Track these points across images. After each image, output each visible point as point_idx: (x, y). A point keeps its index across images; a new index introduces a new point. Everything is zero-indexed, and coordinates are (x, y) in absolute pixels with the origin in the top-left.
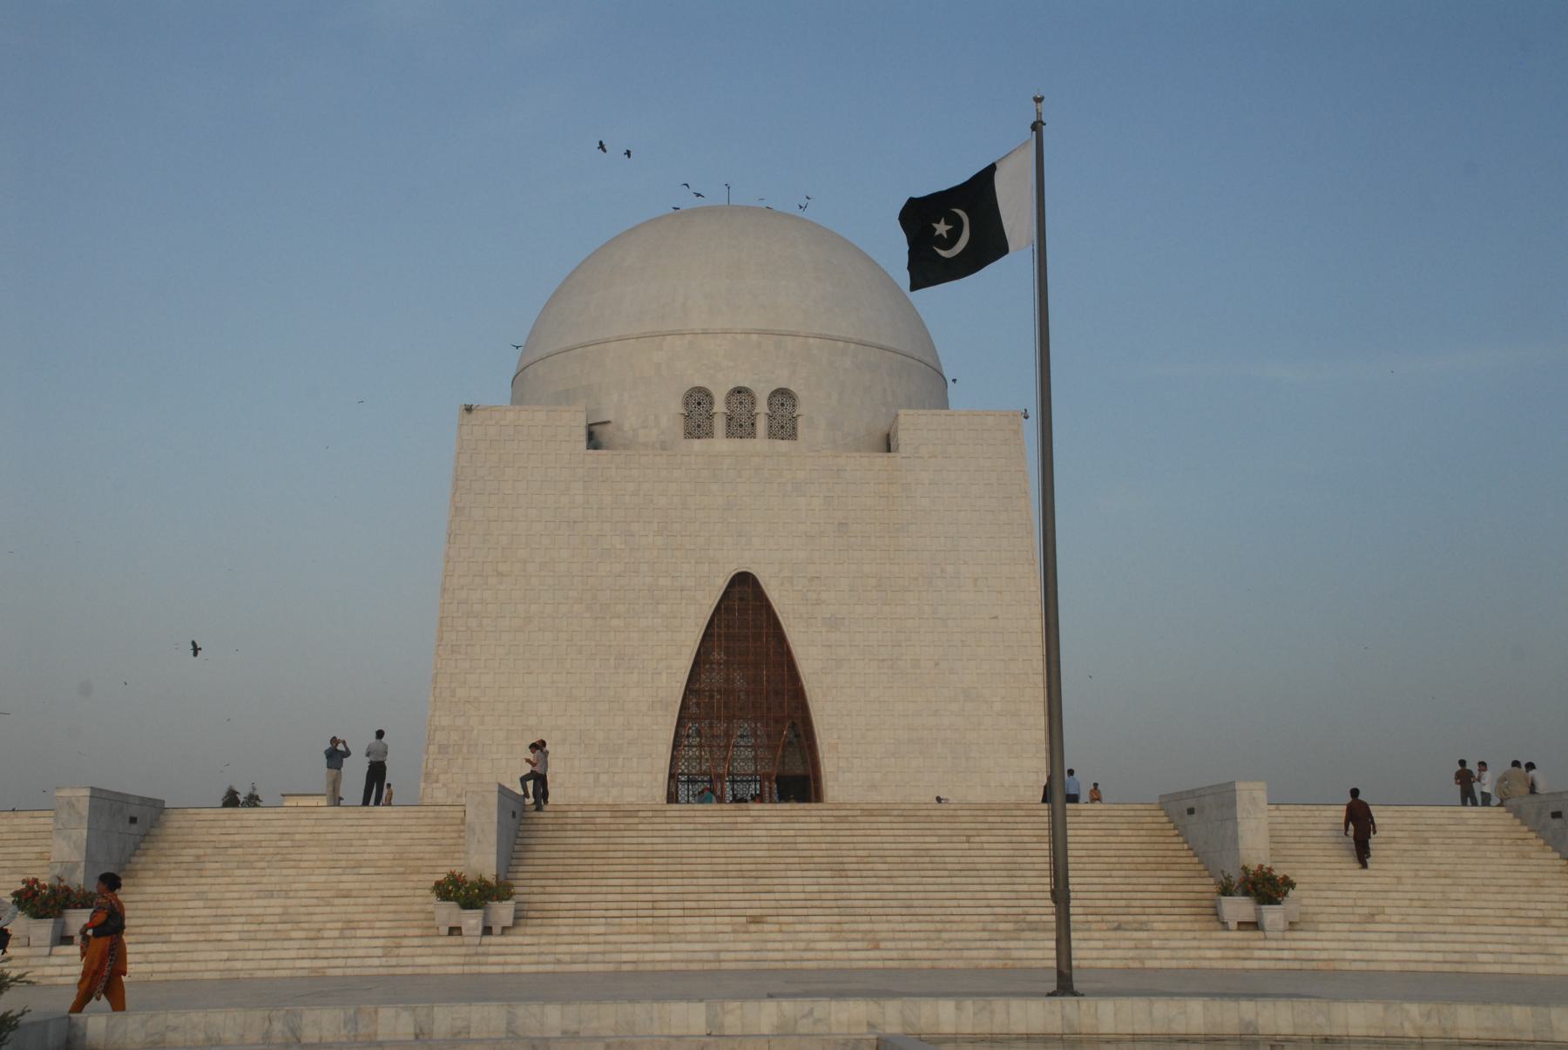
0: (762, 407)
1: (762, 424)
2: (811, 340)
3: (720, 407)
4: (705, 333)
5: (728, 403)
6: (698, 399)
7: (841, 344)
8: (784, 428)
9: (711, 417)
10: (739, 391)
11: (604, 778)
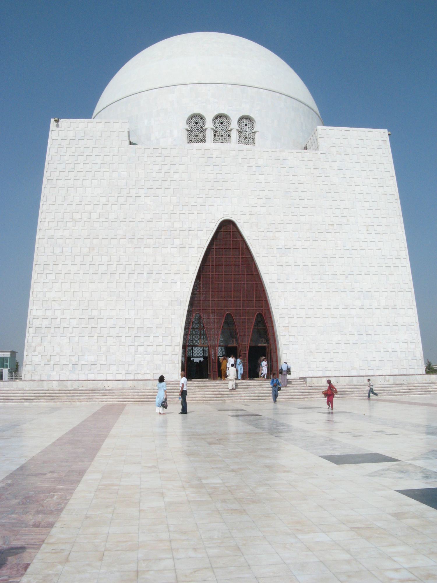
1: (234, 135)
3: (209, 124)
6: (196, 120)
8: (248, 138)
10: (220, 116)
11: (141, 349)
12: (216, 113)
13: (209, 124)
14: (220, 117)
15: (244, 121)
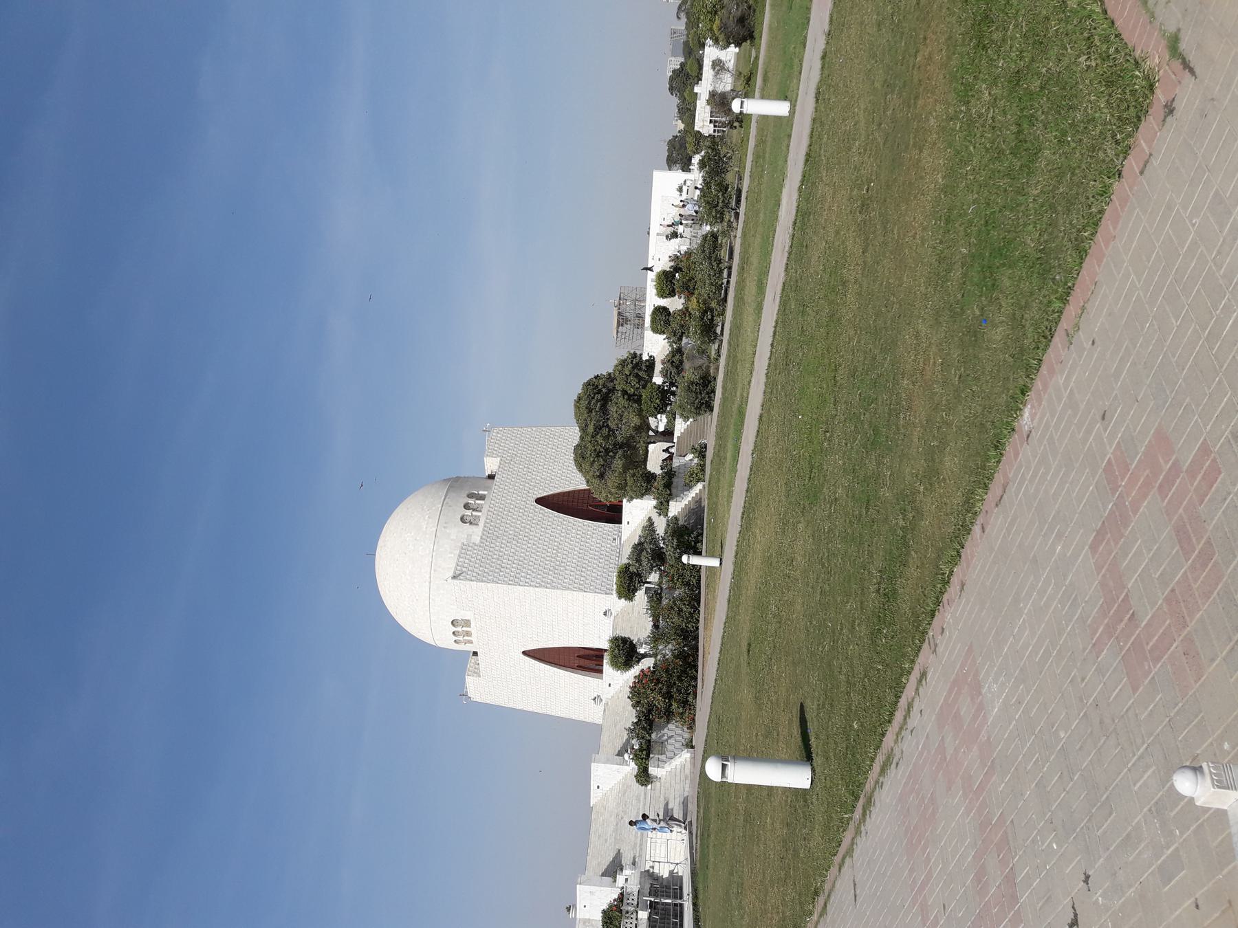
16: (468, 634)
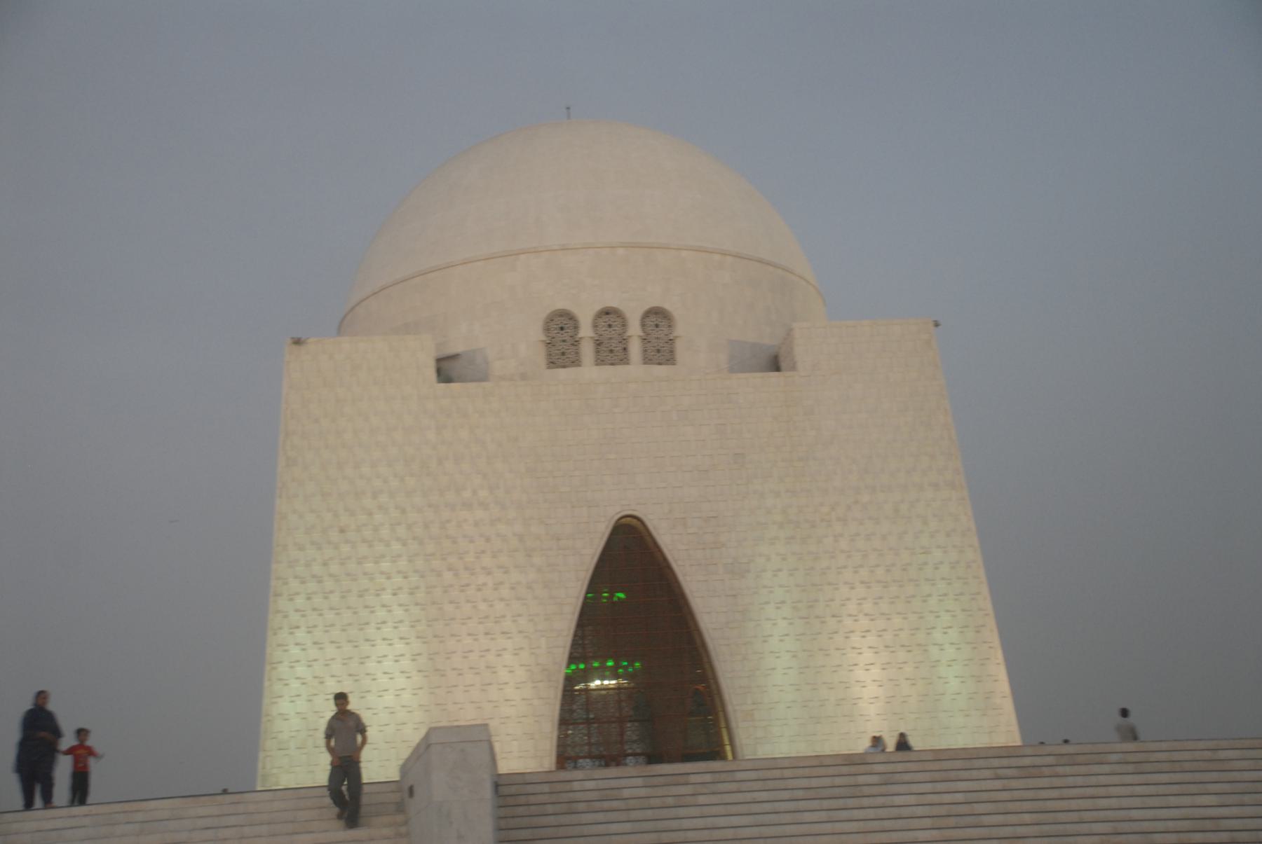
0: (634, 329)
1: (635, 348)
2: (684, 253)
3: (586, 331)
4: (564, 249)
5: (595, 326)
7: (717, 257)
8: (661, 351)
9: (576, 343)
10: (607, 312)
12: (598, 307)
13: (586, 331)
14: (607, 313)
15: (651, 321)
16: (611, 351)
